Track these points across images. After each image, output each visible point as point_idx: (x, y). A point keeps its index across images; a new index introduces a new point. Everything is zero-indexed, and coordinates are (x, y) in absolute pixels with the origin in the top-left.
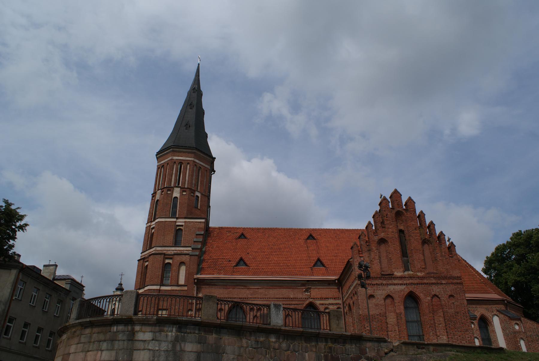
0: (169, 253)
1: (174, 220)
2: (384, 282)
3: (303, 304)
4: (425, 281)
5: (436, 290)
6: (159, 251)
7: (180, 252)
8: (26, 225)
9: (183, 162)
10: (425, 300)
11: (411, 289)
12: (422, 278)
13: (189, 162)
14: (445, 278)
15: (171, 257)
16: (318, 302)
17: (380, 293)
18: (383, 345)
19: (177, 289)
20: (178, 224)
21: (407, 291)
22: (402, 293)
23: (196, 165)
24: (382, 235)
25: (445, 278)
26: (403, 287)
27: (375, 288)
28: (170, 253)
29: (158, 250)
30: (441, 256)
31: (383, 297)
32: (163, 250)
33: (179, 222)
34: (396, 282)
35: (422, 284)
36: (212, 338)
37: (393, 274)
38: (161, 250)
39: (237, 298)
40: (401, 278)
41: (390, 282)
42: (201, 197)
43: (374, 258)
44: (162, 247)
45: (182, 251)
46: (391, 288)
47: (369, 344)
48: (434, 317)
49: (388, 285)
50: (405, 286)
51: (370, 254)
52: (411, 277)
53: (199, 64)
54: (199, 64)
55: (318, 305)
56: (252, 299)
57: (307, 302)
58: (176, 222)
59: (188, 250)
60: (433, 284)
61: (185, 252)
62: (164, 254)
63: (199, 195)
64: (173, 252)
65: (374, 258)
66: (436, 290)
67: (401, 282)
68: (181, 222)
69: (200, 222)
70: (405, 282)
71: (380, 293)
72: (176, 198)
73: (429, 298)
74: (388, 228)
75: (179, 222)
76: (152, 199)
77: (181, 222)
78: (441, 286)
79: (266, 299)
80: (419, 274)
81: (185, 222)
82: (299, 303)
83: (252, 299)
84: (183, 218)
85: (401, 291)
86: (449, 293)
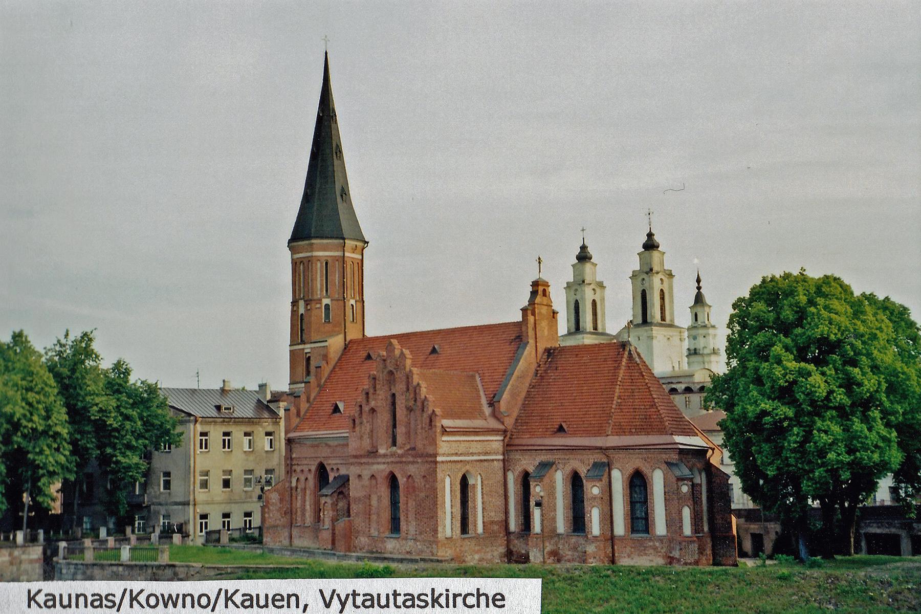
2: (370, 460)
4: (404, 459)
5: (412, 469)
10: (402, 480)
11: (391, 469)
12: (401, 456)
20: (306, 351)
21: (388, 471)
22: (384, 473)
23: (319, 260)
24: (373, 404)
27: (362, 467)
30: (422, 428)
31: (369, 477)
34: (380, 460)
35: (401, 462)
40: (385, 456)
41: (375, 461)
43: (364, 433)
46: (375, 467)
48: (407, 501)
49: (373, 464)
50: (386, 466)
52: (393, 455)
53: (326, 53)
54: (326, 53)
60: (409, 462)
65: (364, 433)
66: (412, 469)
67: (383, 460)
70: (387, 460)
71: (366, 473)
73: (405, 479)
74: (378, 395)
76: (293, 311)
78: (416, 466)
81: (311, 348)
85: (383, 471)
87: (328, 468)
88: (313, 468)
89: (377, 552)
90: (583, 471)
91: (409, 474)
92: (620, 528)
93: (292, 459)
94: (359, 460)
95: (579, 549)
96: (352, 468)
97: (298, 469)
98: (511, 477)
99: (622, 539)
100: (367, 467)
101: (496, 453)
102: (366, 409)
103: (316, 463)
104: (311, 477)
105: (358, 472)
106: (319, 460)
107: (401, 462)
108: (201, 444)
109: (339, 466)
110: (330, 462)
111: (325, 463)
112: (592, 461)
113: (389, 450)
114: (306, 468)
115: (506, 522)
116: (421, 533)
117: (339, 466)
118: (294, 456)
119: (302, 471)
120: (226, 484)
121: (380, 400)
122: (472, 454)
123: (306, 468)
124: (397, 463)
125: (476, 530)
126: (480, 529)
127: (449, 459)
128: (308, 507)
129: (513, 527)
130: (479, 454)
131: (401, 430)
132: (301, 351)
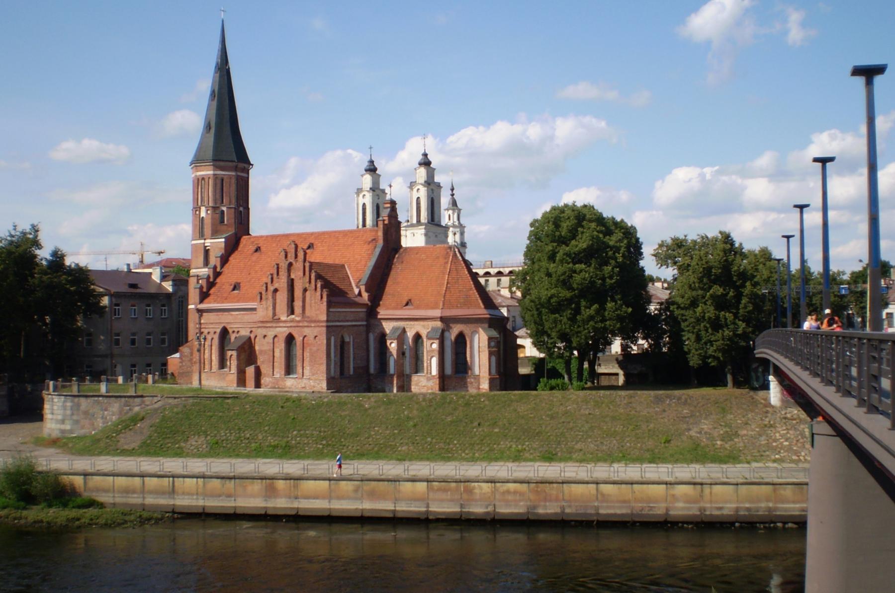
1: (202, 241)
2: (274, 325)
5: (307, 331)
8: (190, 166)
9: (205, 177)
10: (299, 339)
12: (299, 322)
14: (315, 321)
17: (271, 333)
18: (155, 398)
20: (206, 245)
21: (288, 333)
24: (276, 285)
25: (315, 321)
26: (286, 329)
30: (315, 303)
34: (281, 325)
35: (298, 327)
36: (76, 400)
37: (279, 319)
40: (285, 322)
41: (278, 325)
42: (227, 211)
46: (278, 329)
47: (147, 398)
49: (276, 327)
51: (267, 302)
52: (292, 321)
53: (223, 21)
54: (223, 21)
58: (204, 243)
62: (198, 276)
63: (224, 209)
66: (307, 331)
67: (284, 325)
68: (208, 242)
71: (271, 333)
72: (203, 217)
74: (282, 279)
77: (208, 242)
78: (310, 329)
80: (298, 319)
85: (285, 332)
86: (315, 334)
87: (230, 331)
88: (218, 331)
89: (279, 388)
90: (424, 333)
91: (305, 334)
92: (449, 370)
93: (200, 324)
94: (265, 325)
95: (420, 384)
96: (259, 330)
97: (206, 331)
98: (372, 337)
99: (449, 377)
100: (271, 329)
101: (362, 321)
102: (271, 288)
103: (221, 327)
104: (216, 337)
105: (265, 333)
107: (298, 327)
108: (119, 312)
109: (240, 329)
110: (232, 326)
111: (228, 327)
112: (430, 327)
113: (289, 318)
115: (367, 367)
116: (313, 375)
117: (240, 329)
118: (202, 321)
119: (209, 333)
120: (133, 342)
121: (282, 283)
122: (348, 321)
123: (212, 331)
124: (294, 327)
125: (349, 372)
126: (352, 372)
127: (354, 323)
128: (214, 358)
129: (372, 370)
130: (351, 321)
131: (298, 304)
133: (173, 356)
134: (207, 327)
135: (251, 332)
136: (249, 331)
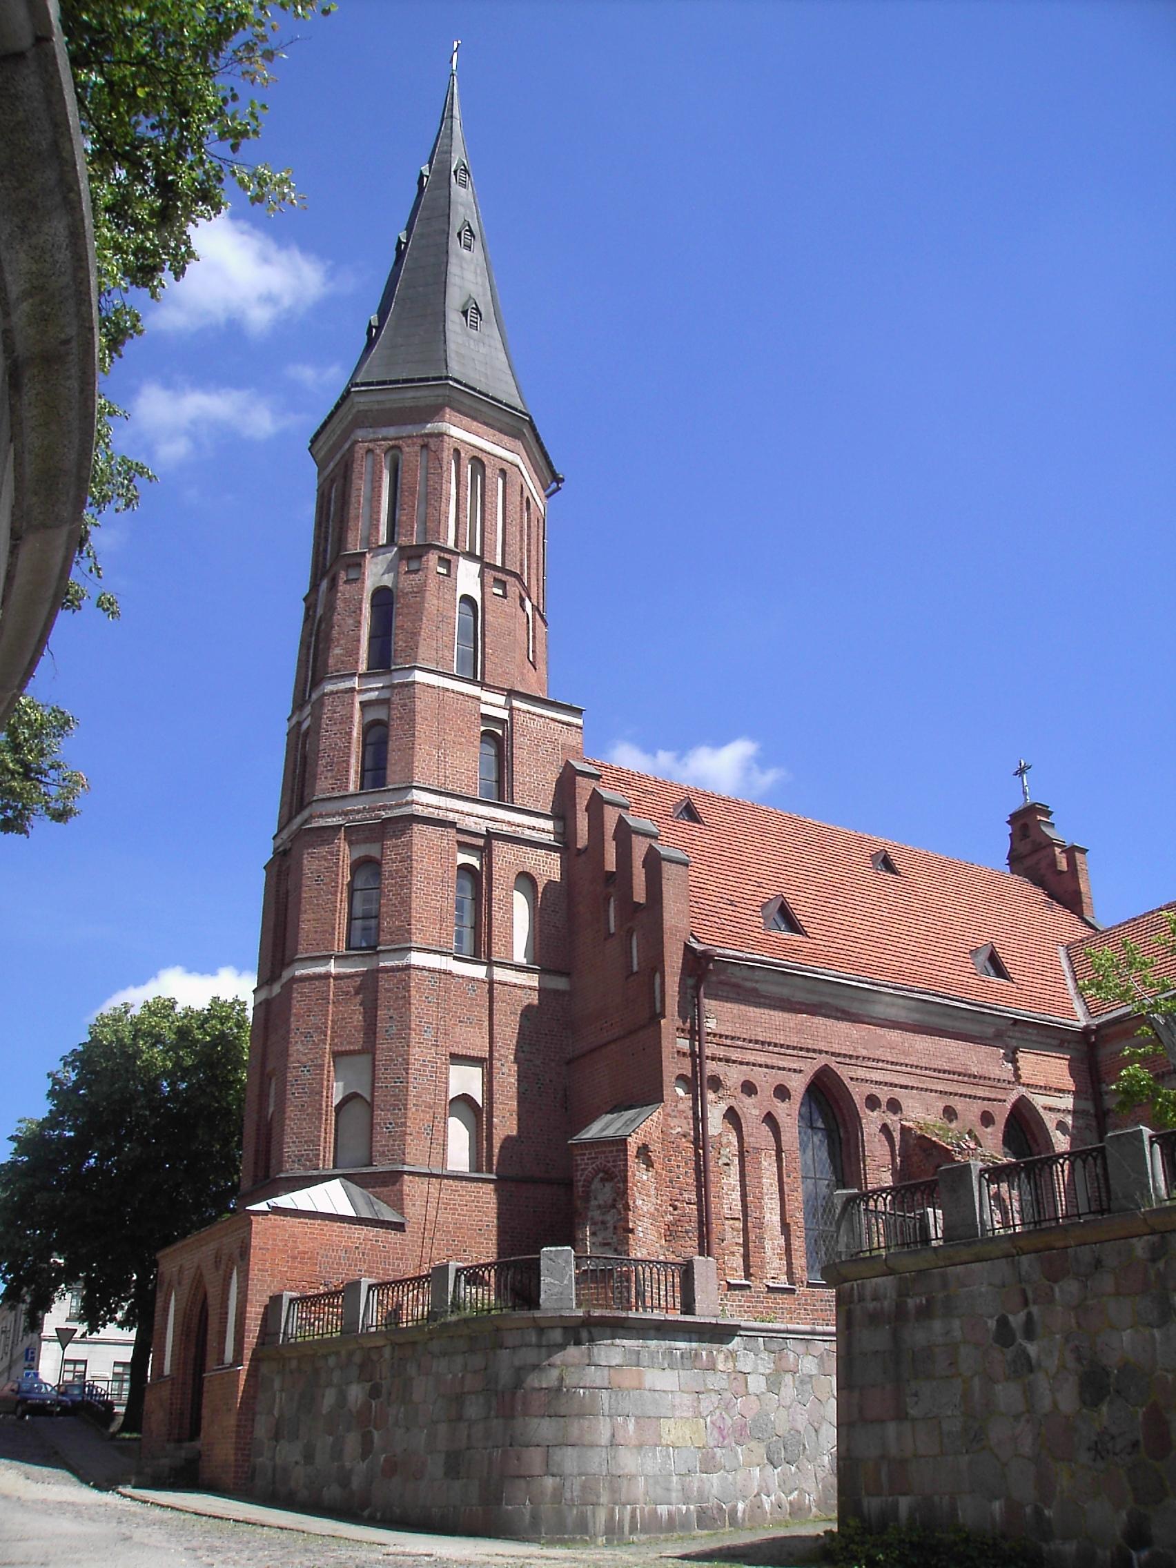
0: (469, 823)
1: (474, 690)
3: (1005, 1101)
6: (431, 810)
7: (509, 829)
13: (506, 466)
15: (481, 842)
16: (1039, 1101)
19: (519, 982)
28: (473, 826)
29: (428, 806)
32: (446, 810)
33: (491, 704)
38: (439, 808)
39: (827, 1052)
44: (441, 793)
45: (518, 829)
55: (1041, 1110)
56: (870, 1064)
57: (1013, 1097)
59: (537, 826)
61: (528, 832)
64: (482, 827)
69: (569, 724)
75: (491, 704)
79: (909, 1069)
82: (993, 1096)
83: (870, 1064)
84: (503, 689)
87: (858, 1093)
88: (798, 1085)
97: (733, 1076)
103: (810, 1067)
104: (788, 1114)
106: (822, 1060)
109: (898, 1093)
110: (861, 1073)
111: (844, 1072)
114: (765, 1081)
117: (898, 1093)
119: (749, 1088)
123: (765, 1081)
132: (470, 704)
133: (284, 1201)
134: (735, 1055)
135: (950, 1113)
136: (941, 1105)
